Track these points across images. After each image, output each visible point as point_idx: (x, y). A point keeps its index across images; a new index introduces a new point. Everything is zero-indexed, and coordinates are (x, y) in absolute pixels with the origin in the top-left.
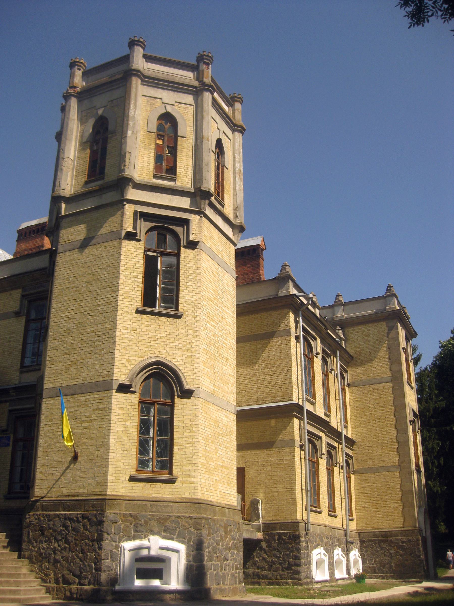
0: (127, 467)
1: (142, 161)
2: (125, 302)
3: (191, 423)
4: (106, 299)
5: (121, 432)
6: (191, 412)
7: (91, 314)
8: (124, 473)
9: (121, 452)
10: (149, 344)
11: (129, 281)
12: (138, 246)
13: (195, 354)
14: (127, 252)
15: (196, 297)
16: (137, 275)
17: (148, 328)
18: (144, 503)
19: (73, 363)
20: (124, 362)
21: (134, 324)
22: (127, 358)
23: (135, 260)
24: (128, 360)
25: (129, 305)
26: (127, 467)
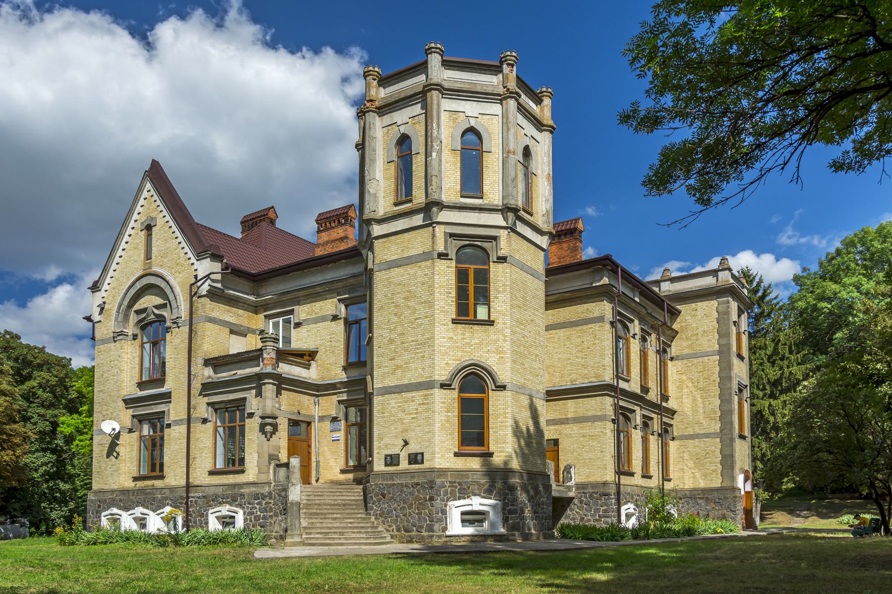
19: (398, 367)
24: (447, 364)
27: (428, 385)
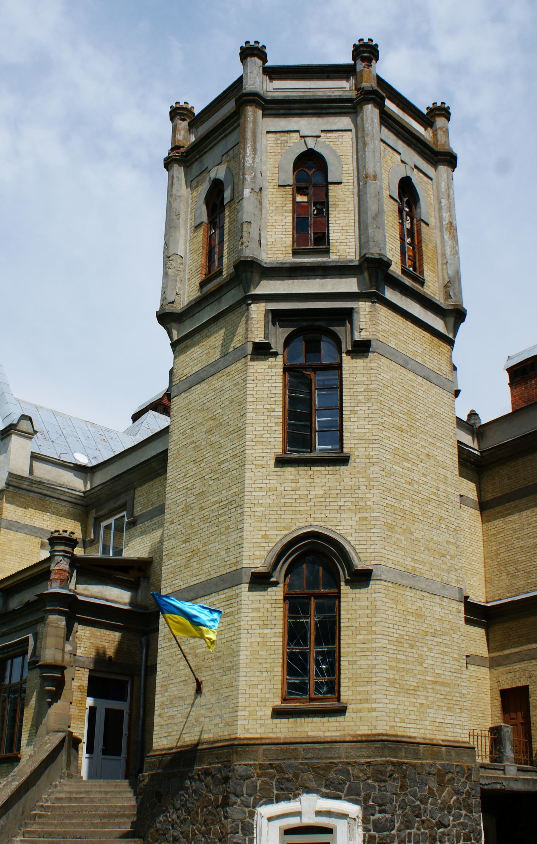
0: (267, 696)
1: (273, 233)
2: (257, 451)
3: (369, 619)
4: (231, 451)
5: (256, 644)
6: (368, 604)
7: (213, 478)
8: (263, 704)
9: (258, 674)
10: (297, 509)
11: (262, 417)
12: (273, 364)
13: (372, 515)
14: (256, 374)
15: (370, 427)
16: (273, 406)
17: (294, 485)
18: (292, 747)
20: (259, 541)
21: (272, 481)
22: (263, 533)
23: (269, 385)
24: (265, 536)
25: (263, 455)
26: (267, 696)
27: (228, 581)
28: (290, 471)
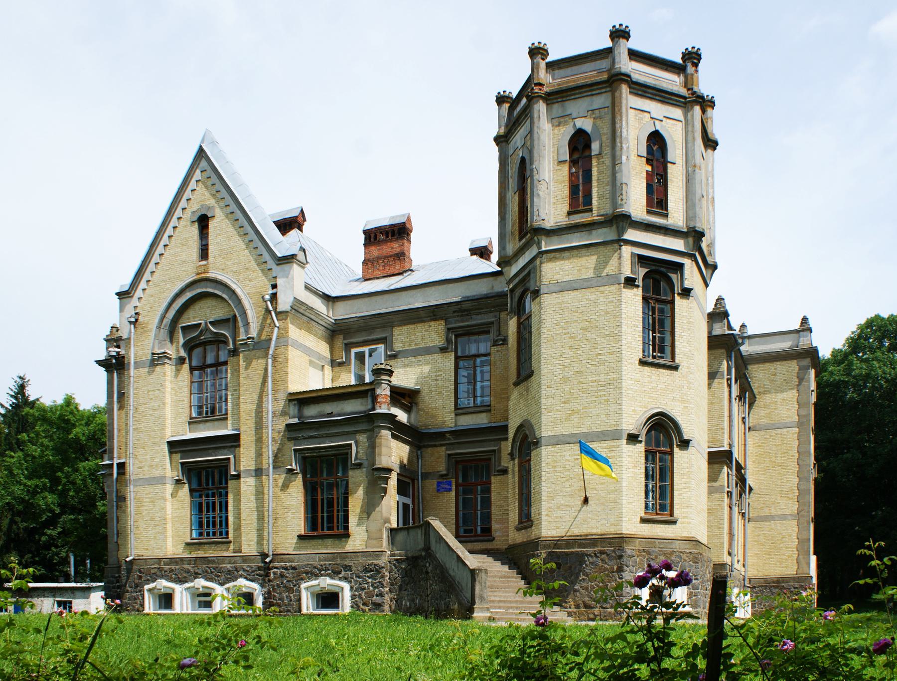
19: (573, 412)
28: (647, 369)
